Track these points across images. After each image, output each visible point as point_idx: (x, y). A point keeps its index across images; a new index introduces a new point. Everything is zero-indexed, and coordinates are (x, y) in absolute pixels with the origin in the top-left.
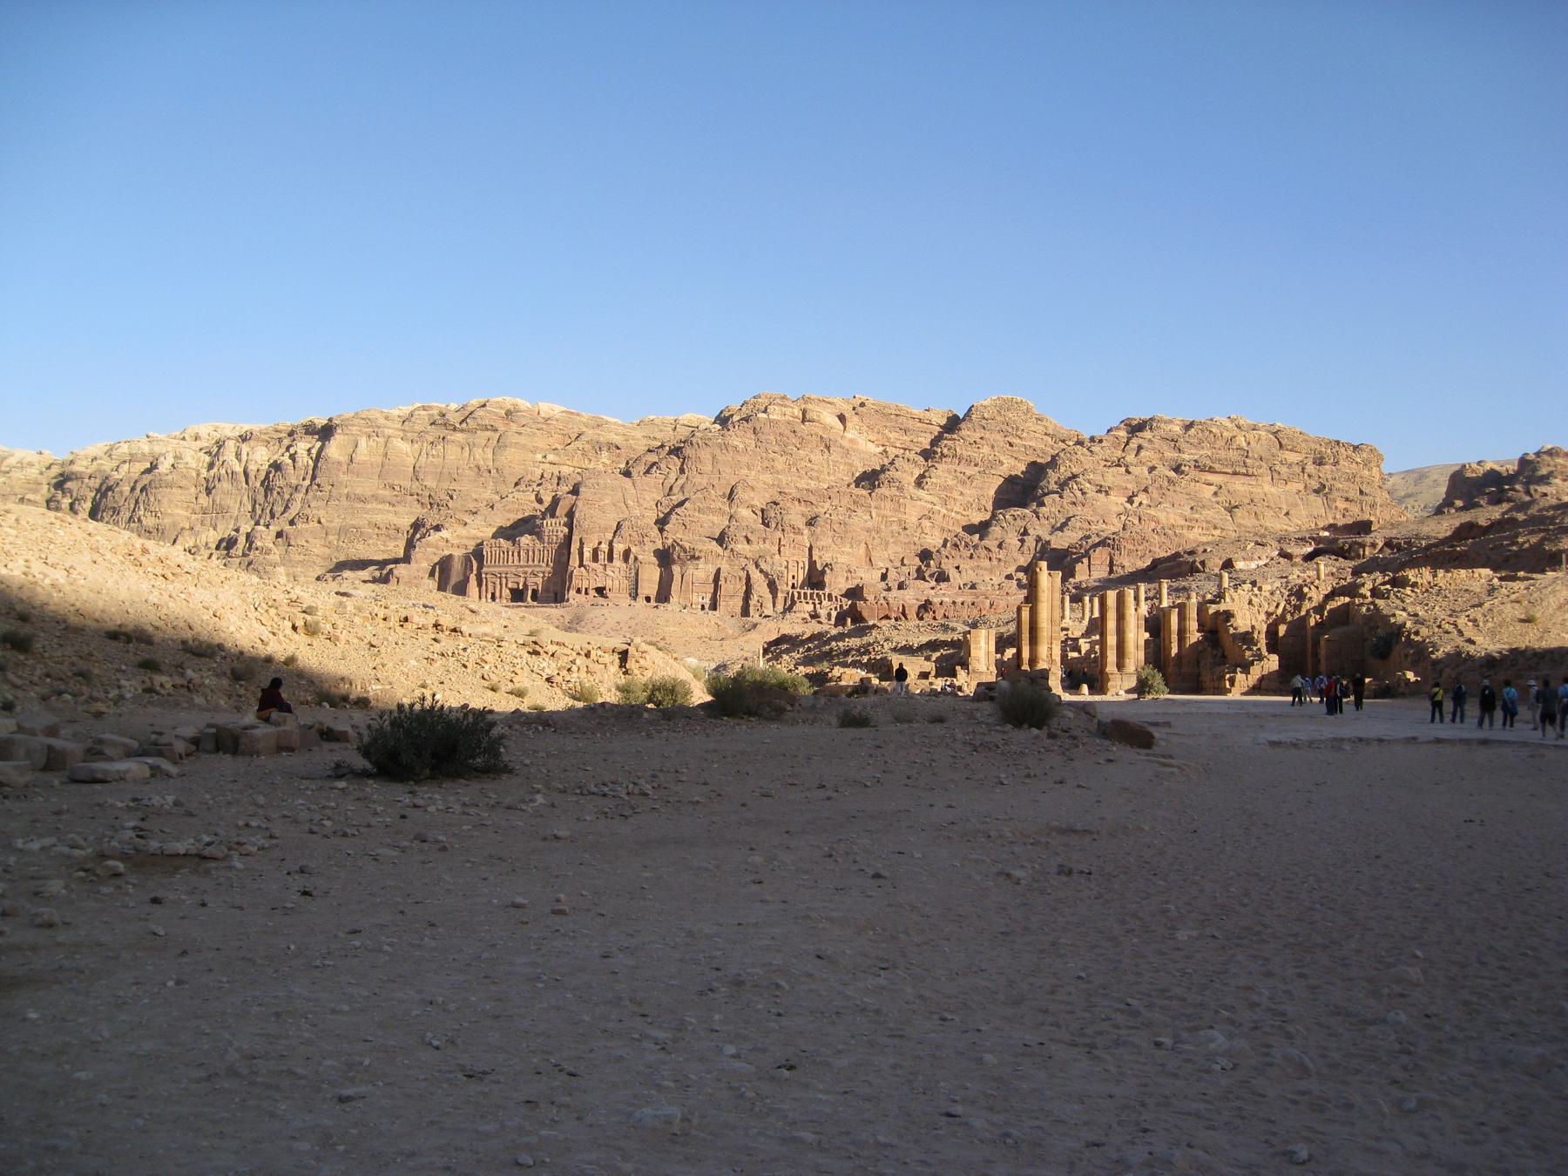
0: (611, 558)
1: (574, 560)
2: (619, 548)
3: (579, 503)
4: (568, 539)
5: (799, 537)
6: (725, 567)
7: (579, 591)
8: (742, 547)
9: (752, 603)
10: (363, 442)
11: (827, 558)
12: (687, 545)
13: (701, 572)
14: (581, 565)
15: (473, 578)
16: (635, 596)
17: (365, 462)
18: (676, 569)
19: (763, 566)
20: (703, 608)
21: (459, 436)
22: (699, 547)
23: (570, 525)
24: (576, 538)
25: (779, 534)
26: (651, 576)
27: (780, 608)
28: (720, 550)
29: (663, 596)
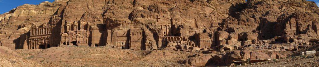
0: (79, 29)
1: (63, 30)
2: (83, 23)
3: (67, 8)
4: (61, 21)
5: (166, 15)
6: (132, 28)
7: (64, 43)
8: (139, 19)
9: (147, 44)
10: (23, 12)
11: (179, 23)
12: (113, 19)
13: (121, 31)
14: (66, 32)
15: (26, 42)
16: (90, 44)
17: (22, 17)
18: (109, 31)
19: (151, 27)
20: (123, 48)
21: (51, 8)
22: (119, 19)
23: (62, 16)
24: (63, 21)
25: (157, 14)
26: (97, 35)
27: (160, 45)
28: (130, 21)
29: (103, 42)
